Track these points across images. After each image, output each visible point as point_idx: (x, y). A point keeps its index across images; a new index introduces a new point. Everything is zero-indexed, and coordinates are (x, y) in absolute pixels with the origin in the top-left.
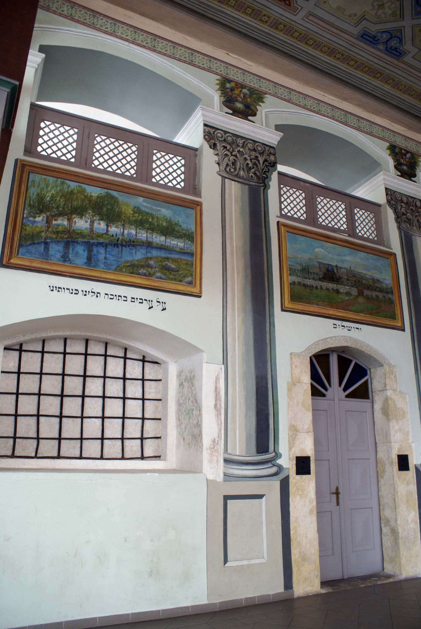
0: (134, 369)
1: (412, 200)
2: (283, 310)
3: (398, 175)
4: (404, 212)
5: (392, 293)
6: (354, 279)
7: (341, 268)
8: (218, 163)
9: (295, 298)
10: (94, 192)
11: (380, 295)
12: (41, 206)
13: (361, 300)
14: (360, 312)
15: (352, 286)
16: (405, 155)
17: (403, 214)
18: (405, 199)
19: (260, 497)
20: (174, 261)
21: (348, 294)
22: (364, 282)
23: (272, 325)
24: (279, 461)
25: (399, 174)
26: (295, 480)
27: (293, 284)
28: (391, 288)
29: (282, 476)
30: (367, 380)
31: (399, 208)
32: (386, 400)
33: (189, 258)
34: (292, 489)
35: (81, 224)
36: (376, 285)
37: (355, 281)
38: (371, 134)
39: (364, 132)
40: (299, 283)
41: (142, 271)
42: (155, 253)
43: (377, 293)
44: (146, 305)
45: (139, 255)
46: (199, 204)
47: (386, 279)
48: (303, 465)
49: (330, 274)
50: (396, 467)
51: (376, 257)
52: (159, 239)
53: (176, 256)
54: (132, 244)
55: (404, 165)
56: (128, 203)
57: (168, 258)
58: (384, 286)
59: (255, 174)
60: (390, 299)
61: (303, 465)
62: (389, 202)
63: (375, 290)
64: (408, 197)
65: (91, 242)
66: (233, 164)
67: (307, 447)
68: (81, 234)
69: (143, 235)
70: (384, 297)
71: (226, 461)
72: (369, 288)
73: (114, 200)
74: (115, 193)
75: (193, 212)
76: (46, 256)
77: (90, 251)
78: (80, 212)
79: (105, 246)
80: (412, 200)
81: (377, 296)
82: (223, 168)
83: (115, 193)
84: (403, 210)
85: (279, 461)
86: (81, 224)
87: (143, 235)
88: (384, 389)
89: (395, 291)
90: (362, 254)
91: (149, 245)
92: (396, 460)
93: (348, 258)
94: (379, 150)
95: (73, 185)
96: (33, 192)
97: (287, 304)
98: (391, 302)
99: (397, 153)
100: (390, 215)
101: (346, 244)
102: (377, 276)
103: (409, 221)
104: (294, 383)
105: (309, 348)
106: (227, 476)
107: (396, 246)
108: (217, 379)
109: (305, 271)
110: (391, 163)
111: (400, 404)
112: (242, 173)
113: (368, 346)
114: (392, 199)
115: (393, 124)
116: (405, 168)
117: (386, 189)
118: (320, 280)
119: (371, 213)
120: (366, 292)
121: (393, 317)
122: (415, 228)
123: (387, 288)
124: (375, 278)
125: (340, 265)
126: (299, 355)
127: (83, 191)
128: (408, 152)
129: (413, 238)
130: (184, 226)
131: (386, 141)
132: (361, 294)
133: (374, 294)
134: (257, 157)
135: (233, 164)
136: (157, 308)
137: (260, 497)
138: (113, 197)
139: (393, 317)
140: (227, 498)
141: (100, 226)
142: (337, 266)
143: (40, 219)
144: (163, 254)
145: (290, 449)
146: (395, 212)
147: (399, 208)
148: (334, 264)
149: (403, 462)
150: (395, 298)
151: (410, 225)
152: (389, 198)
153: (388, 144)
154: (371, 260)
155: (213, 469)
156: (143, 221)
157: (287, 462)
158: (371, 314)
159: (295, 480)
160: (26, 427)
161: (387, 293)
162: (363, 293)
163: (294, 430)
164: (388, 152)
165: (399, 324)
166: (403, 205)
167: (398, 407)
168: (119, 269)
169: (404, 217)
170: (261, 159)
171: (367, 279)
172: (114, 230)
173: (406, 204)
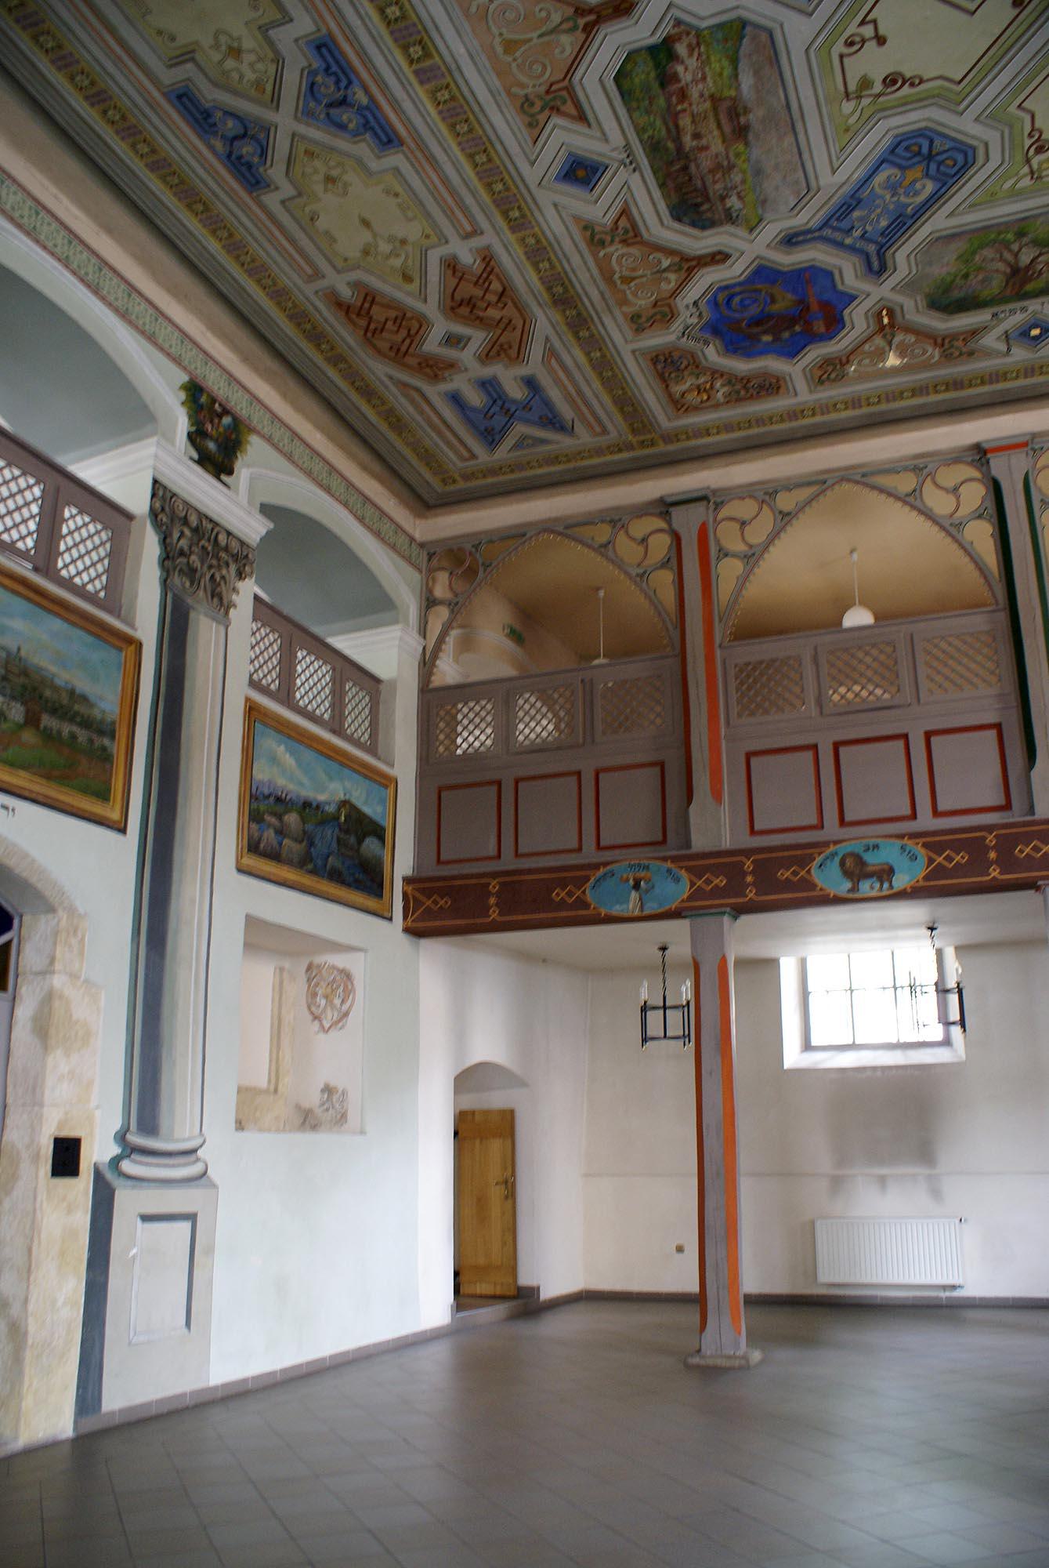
1: (210, 526)
3: (191, 458)
4: (186, 548)
5: (112, 736)
6: (22, 680)
11: (82, 735)
13: (29, 736)
14: (23, 767)
15: (13, 698)
16: (220, 416)
17: (182, 553)
18: (193, 520)
22: (48, 693)
25: (196, 456)
28: (113, 723)
30: (9, 943)
31: (176, 535)
32: (49, 998)
36: (76, 707)
37: (24, 687)
38: (151, 338)
39: (136, 328)
43: (75, 729)
47: (107, 701)
51: (90, 639)
55: (211, 438)
58: (96, 713)
60: (104, 749)
62: (154, 514)
63: (72, 720)
64: (202, 516)
70: (91, 741)
72: (56, 710)
80: (210, 526)
81: (73, 737)
84: (183, 543)
88: (48, 971)
89: (122, 733)
90: (57, 624)
92: (47, 1149)
93: (18, 624)
94: (162, 386)
98: (106, 757)
99: (201, 407)
100: (150, 546)
101: (20, 589)
102: (83, 685)
103: (191, 573)
107: (146, 620)
110: (182, 424)
111: (81, 1010)
113: (26, 855)
114: (163, 509)
115: (209, 335)
116: (211, 446)
117: (155, 482)
119: (105, 528)
120: (46, 720)
121: (104, 795)
122: (201, 593)
123: (102, 721)
124: (78, 691)
128: (226, 412)
129: (192, 615)
131: (185, 369)
132: (32, 720)
133: (67, 729)
139: (104, 795)
146: (164, 541)
147: (176, 535)
149: (66, 1157)
150: (118, 749)
151: (192, 583)
152: (158, 505)
153: (185, 378)
154: (79, 642)
158: (48, 777)
161: (101, 733)
162: (38, 720)
164: (183, 396)
165: (115, 816)
166: (187, 532)
167: (75, 1017)
169: (182, 560)
171: (56, 689)
173: (195, 530)
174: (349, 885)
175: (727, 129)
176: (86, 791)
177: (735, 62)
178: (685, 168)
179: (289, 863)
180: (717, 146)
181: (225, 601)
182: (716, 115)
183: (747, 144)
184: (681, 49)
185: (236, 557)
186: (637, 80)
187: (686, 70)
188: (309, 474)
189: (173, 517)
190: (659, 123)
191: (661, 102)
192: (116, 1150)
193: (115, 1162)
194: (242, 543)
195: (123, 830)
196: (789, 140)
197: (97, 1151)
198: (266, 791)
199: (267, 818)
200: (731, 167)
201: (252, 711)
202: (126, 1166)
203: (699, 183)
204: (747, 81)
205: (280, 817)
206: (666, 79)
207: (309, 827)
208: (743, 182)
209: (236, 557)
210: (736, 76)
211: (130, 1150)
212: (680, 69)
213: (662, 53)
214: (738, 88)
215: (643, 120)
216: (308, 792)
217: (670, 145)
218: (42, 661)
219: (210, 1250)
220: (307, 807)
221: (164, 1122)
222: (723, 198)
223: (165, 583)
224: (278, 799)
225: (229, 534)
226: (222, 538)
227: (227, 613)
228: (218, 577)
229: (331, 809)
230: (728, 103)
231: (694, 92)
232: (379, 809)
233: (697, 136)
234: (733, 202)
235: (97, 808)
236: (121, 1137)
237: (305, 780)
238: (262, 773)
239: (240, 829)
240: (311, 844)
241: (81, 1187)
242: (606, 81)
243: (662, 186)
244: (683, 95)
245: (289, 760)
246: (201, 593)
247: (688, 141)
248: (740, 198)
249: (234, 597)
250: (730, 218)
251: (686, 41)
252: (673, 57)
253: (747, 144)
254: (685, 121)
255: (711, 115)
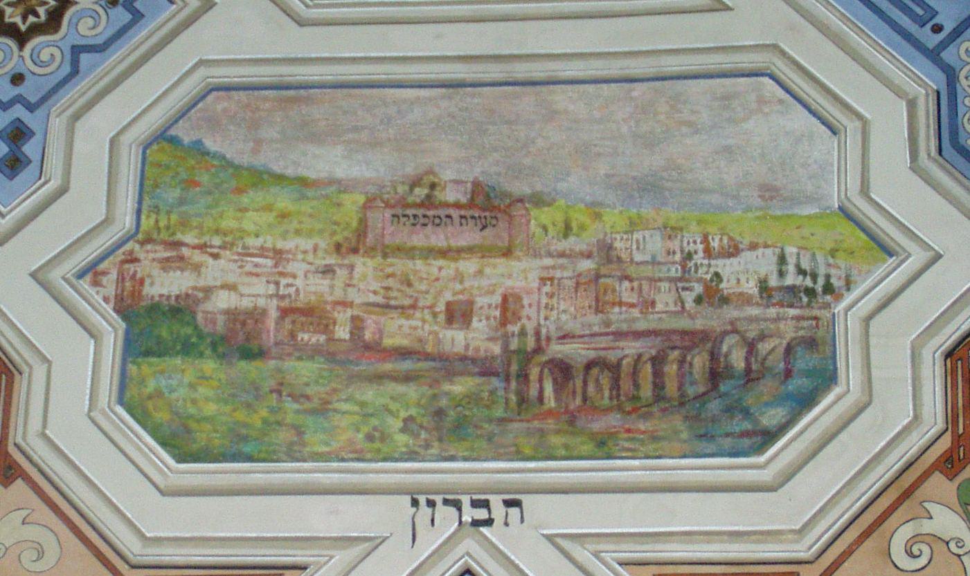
175: (469, 236)
177: (261, 178)
178: (562, 370)
180: (519, 274)
182: (408, 252)
183: (539, 200)
184: (166, 285)
186: (211, 409)
187: (231, 286)
190: (369, 394)
191: (304, 371)
196: (561, 97)
200: (606, 251)
203: (631, 348)
204: (326, 162)
206: (240, 340)
208: (671, 231)
210: (303, 182)
212: (223, 301)
213: (154, 329)
214: (344, 186)
215: (346, 425)
217: (459, 387)
222: (713, 295)
230: (380, 219)
231: (308, 286)
233: (459, 314)
234: (742, 274)
242: (176, 481)
243: (604, 447)
244: (311, 314)
247: (476, 337)
248: (733, 251)
250: (816, 292)
251: (147, 265)
252: (181, 309)
253: (539, 200)
254: (397, 331)
255: (399, 265)
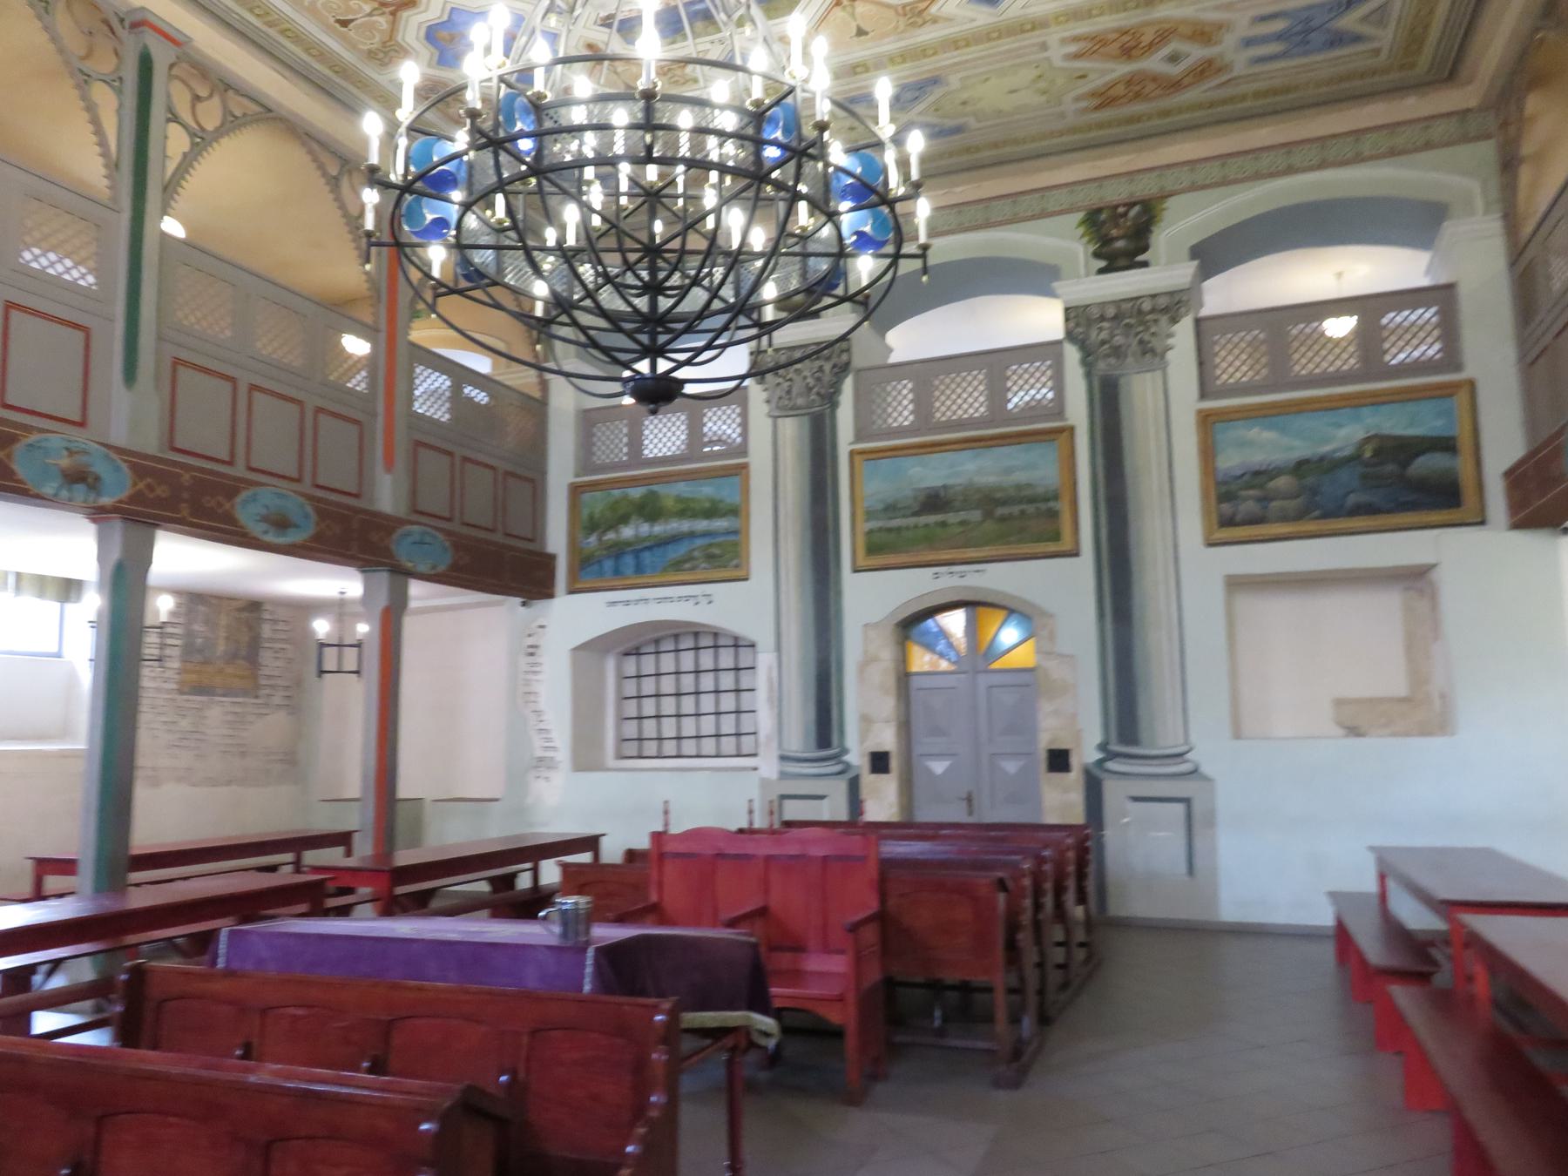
0: (726, 659)
2: (856, 571)
3: (1101, 271)
7: (952, 487)
8: (768, 402)
9: (873, 549)
10: (636, 493)
11: (1030, 509)
12: (593, 526)
13: (990, 526)
16: (1125, 214)
17: (1103, 343)
19: (821, 797)
20: (719, 545)
21: (963, 523)
22: (998, 495)
23: (839, 593)
24: (847, 758)
25: (1102, 264)
26: (869, 780)
27: (870, 533)
29: (851, 774)
33: (732, 538)
34: (865, 793)
35: (627, 532)
40: (880, 530)
41: (687, 566)
42: (699, 542)
43: (1024, 507)
44: (692, 601)
45: (680, 550)
46: (745, 466)
48: (879, 762)
49: (934, 502)
50: (1043, 765)
52: (702, 525)
53: (721, 539)
54: (675, 539)
56: (670, 493)
57: (711, 545)
58: (1040, 490)
59: (818, 394)
61: (879, 762)
64: (1117, 303)
65: (638, 549)
66: (789, 392)
67: (886, 739)
68: (628, 543)
69: (685, 526)
71: (783, 758)
72: (1004, 502)
73: (653, 496)
74: (655, 488)
75: (736, 479)
76: (601, 574)
77: (637, 557)
78: (624, 520)
79: (649, 548)
82: (773, 405)
83: (655, 488)
84: (1104, 335)
85: (847, 758)
86: (627, 532)
87: (685, 526)
91: (692, 535)
95: (617, 493)
96: (585, 513)
97: (861, 562)
98: (1053, 515)
99: (1104, 222)
100: (1072, 354)
102: (1021, 477)
103: (1117, 352)
104: (868, 661)
105: (892, 614)
106: (783, 775)
107: (1078, 411)
108: (770, 669)
109: (891, 509)
112: (800, 401)
115: (1098, 163)
116: (1120, 244)
118: (916, 514)
120: (1000, 511)
121: (1056, 537)
125: (950, 482)
126: (876, 625)
127: (625, 497)
128: (1131, 205)
129: (1122, 381)
130: (728, 500)
131: (1078, 210)
132: (988, 515)
133: (1016, 510)
134: (821, 369)
135: (789, 392)
136: (704, 601)
137: (821, 797)
138: (653, 493)
140: (784, 797)
141: (645, 529)
142: (945, 487)
143: (593, 539)
144: (706, 541)
145: (862, 740)
147: (1093, 334)
148: (938, 483)
149: (1059, 760)
150: (1063, 506)
152: (1072, 324)
153: (1080, 216)
155: (768, 766)
156: (687, 510)
157: (856, 757)
159: (869, 780)
160: (649, 728)
161: (1047, 500)
163: (866, 720)
165: (1066, 545)
166: (1105, 324)
168: (665, 570)
170: (827, 367)
172: (659, 529)
173: (1115, 318)
174: (1389, 511)
176: (1040, 539)
179: (1284, 518)
181: (1159, 351)
185: (1165, 310)
188: (1258, 176)
189: (1090, 322)
192: (1099, 756)
193: (1100, 762)
194: (1171, 294)
195: (1076, 554)
197: (1087, 753)
198: (1239, 473)
199: (1244, 493)
201: (1207, 421)
202: (1111, 765)
205: (1261, 486)
207: (1310, 480)
209: (1165, 310)
211: (1113, 756)
216: (1301, 449)
218: (990, 480)
219: (1211, 822)
220: (1300, 468)
221: (1144, 735)
223: (1088, 375)
224: (1257, 473)
225: (1153, 296)
226: (1147, 306)
227: (1163, 356)
228: (1147, 337)
229: (1346, 453)
232: (1439, 423)
235: (1052, 547)
236: (1103, 747)
237: (1297, 443)
238: (1231, 461)
239: (1206, 513)
240: (1314, 491)
241: (1075, 777)
245: (1269, 435)
246: (1130, 360)
249: (1170, 341)
